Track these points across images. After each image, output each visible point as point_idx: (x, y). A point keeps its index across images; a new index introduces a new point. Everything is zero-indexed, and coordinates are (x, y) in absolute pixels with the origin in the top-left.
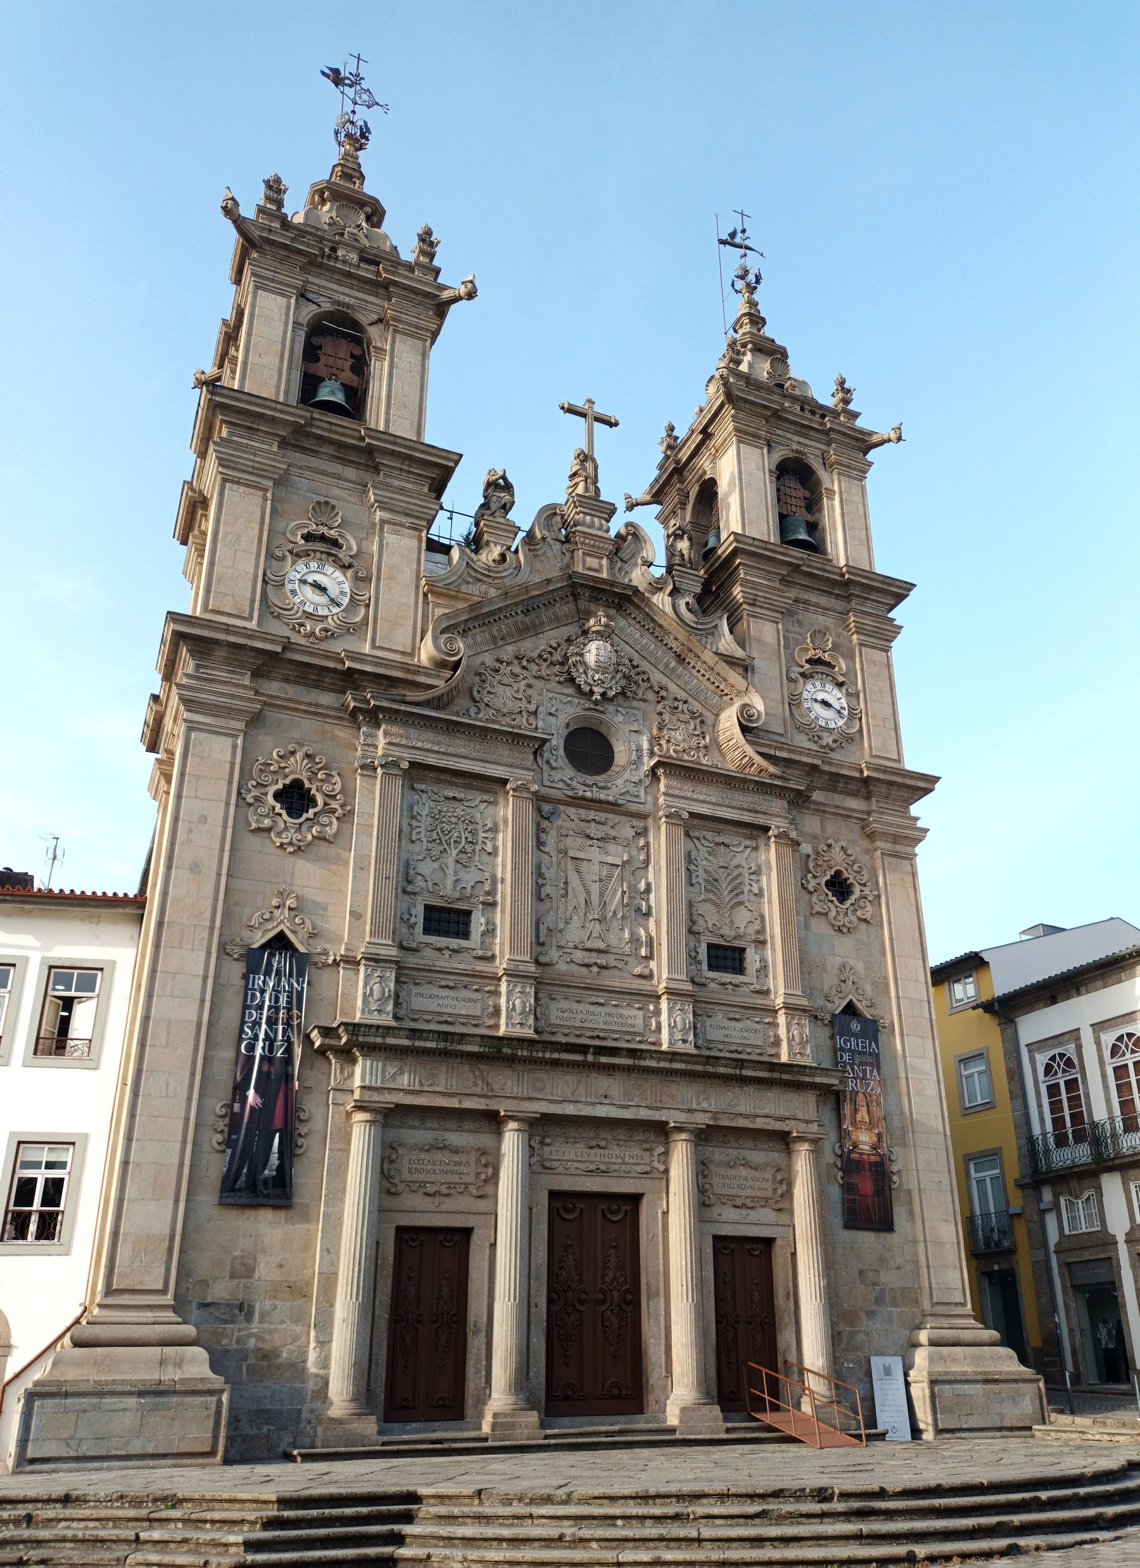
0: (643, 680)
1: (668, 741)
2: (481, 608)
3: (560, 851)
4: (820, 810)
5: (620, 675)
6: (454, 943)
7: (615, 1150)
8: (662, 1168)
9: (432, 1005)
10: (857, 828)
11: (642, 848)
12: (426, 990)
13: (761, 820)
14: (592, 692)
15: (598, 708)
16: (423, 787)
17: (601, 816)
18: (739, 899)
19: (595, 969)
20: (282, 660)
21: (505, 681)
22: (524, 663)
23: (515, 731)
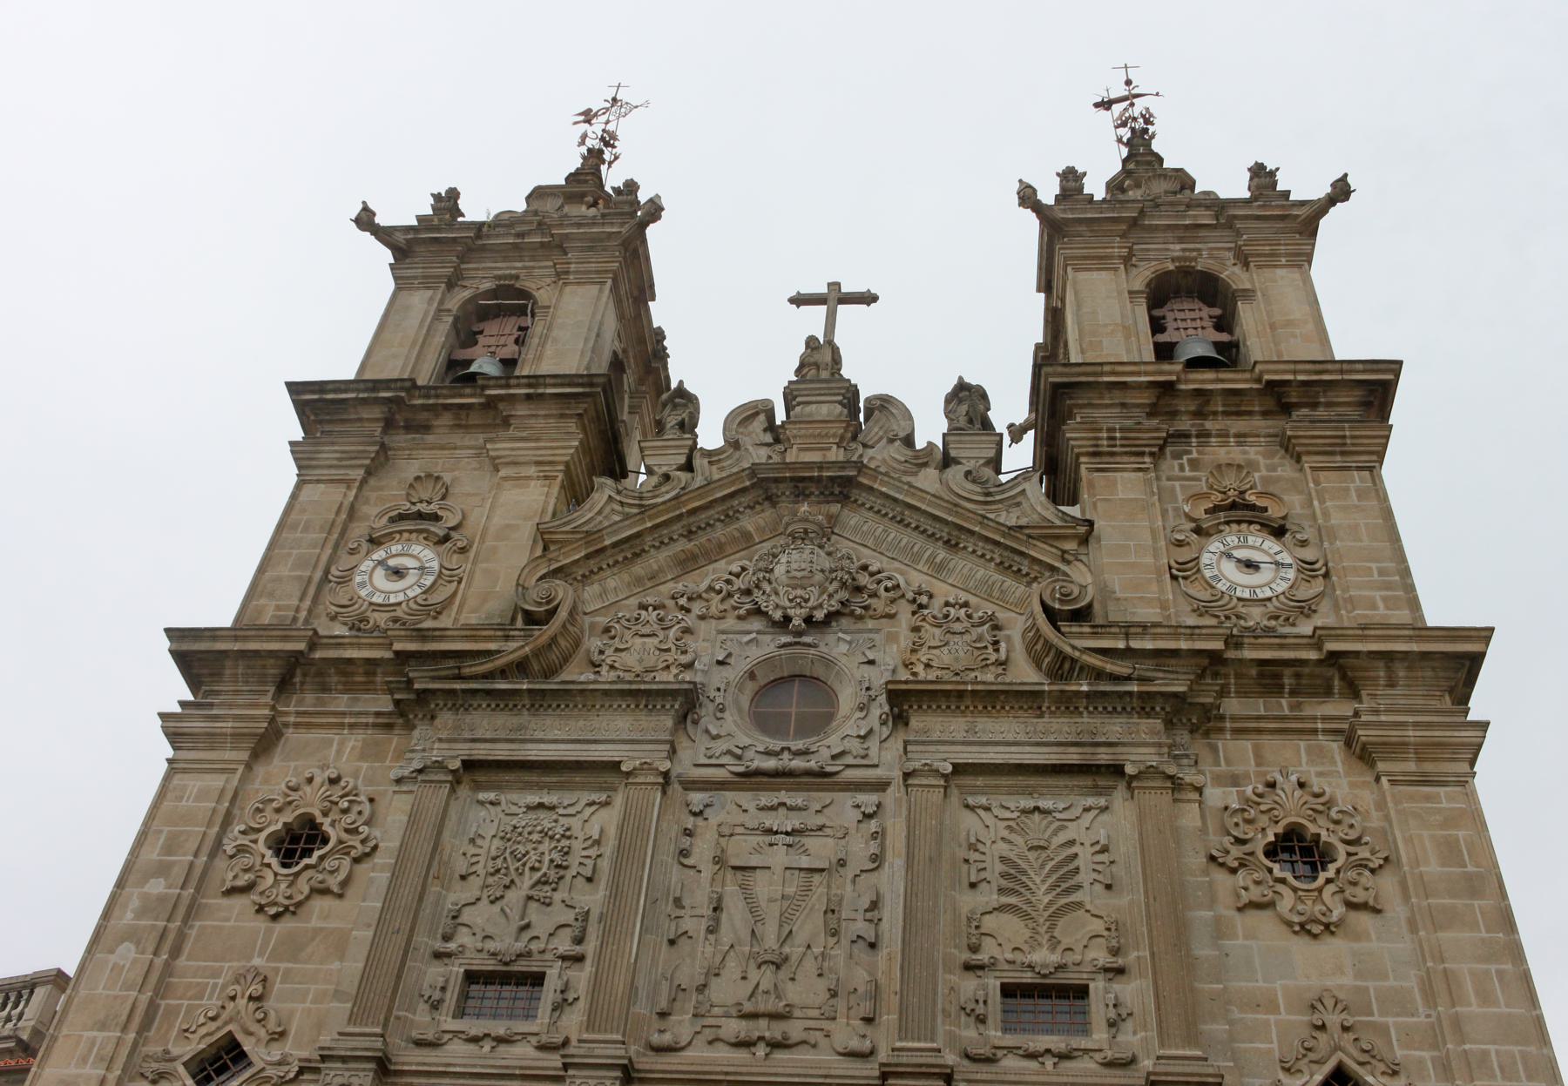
0: (887, 590)
1: (928, 666)
2: (601, 539)
3: (719, 861)
5: (835, 585)
10: (1335, 747)
11: (875, 836)
13: (1104, 756)
15: (807, 639)
16: (492, 796)
17: (796, 799)
18: (1073, 898)
19: (761, 1050)
20: (312, 662)
22: (683, 601)
23: (634, 687)
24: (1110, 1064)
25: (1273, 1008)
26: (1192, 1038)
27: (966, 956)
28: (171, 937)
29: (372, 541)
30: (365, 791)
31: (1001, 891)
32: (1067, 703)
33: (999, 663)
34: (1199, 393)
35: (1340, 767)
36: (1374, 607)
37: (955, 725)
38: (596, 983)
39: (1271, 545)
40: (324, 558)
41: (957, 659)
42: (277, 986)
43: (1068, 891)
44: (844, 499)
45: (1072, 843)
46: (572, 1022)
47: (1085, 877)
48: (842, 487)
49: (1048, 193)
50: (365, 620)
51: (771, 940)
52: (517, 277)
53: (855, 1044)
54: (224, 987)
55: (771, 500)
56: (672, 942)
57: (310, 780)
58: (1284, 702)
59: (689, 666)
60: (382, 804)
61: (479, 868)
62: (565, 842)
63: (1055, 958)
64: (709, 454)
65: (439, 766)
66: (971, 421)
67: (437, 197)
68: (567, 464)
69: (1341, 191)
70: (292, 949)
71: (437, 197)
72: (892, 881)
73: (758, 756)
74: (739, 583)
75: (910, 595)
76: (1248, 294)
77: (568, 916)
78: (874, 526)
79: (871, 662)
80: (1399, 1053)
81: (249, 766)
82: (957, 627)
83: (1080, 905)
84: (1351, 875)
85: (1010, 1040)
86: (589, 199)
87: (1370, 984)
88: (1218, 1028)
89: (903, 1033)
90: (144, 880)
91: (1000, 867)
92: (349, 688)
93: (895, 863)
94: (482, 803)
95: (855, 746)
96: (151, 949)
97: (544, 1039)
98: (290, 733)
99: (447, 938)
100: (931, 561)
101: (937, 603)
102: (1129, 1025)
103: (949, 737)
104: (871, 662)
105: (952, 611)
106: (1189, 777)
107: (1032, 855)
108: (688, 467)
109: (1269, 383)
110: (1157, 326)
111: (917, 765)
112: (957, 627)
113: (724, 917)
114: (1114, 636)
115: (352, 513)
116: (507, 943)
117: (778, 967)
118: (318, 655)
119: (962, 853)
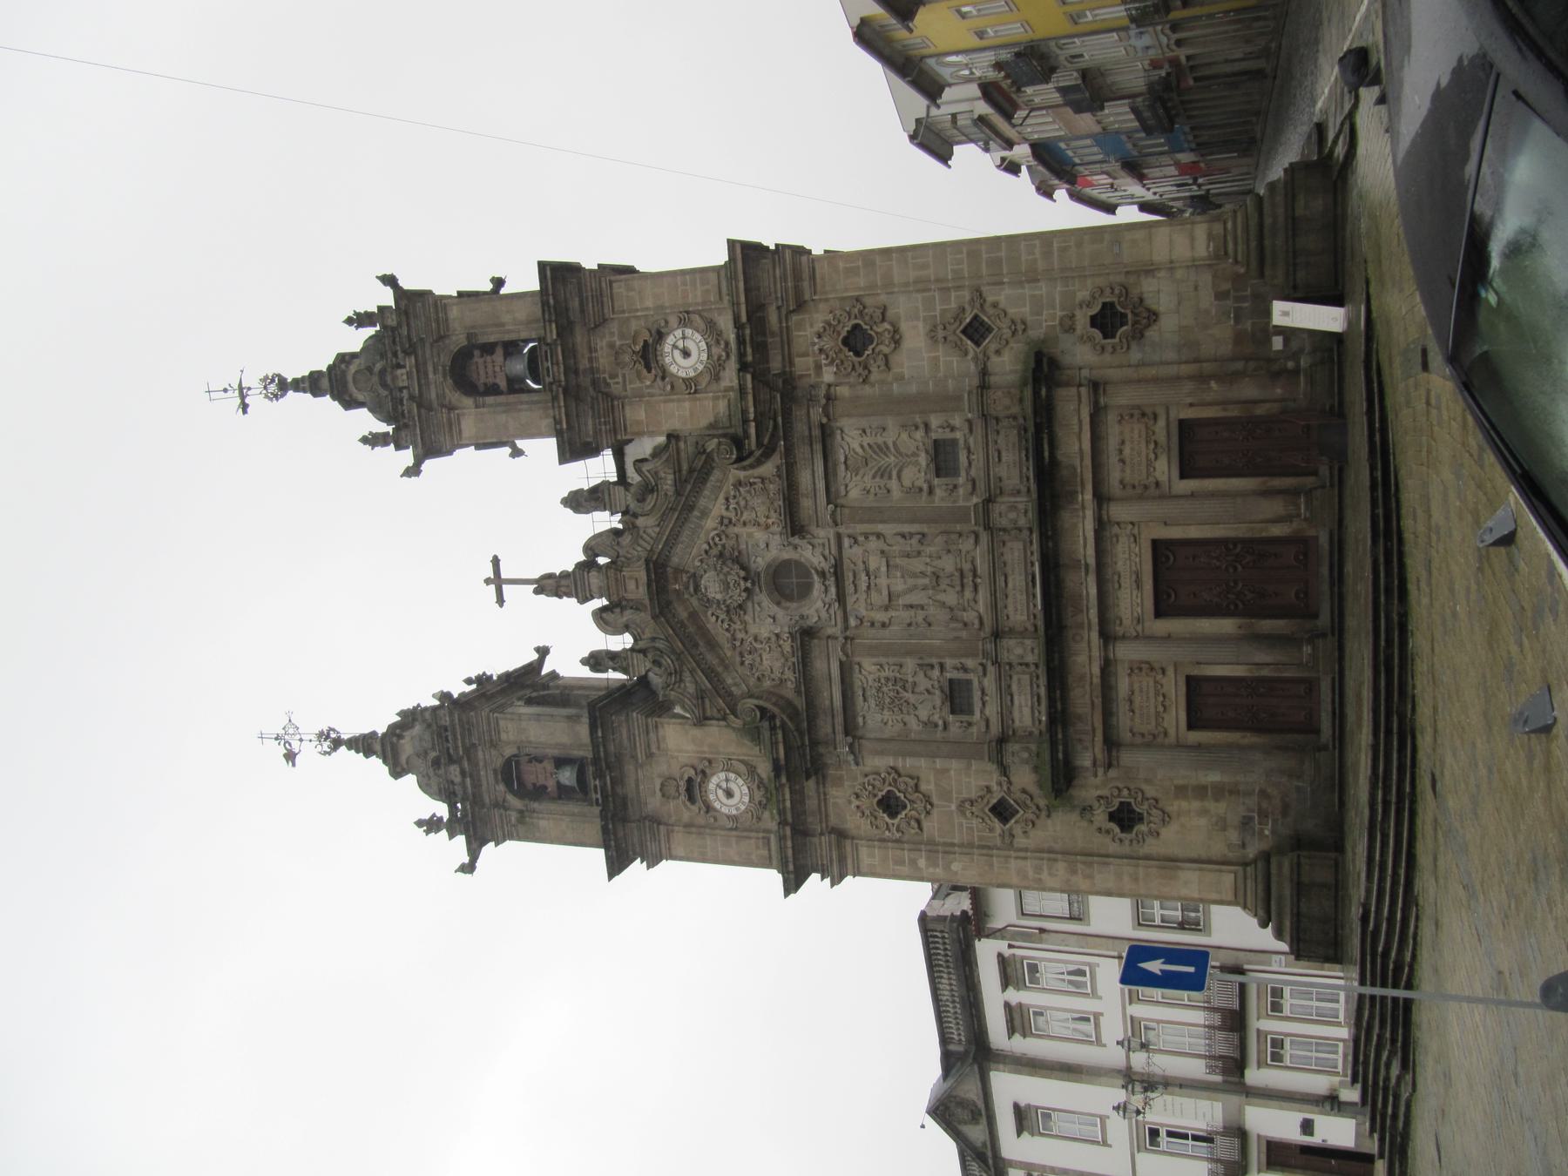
3: (886, 608)
6: (977, 695)
7: (1120, 566)
9: (1027, 711)
10: (795, 318)
12: (1016, 715)
13: (816, 432)
14: (746, 590)
17: (849, 577)
24: (971, 431)
25: (937, 359)
26: (959, 398)
27: (925, 493)
30: (861, 779)
31: (890, 478)
32: (789, 451)
37: (806, 503)
38: (953, 656)
39: (670, 340)
42: (965, 796)
44: (664, 566)
46: (970, 663)
47: (880, 440)
48: (658, 570)
51: (926, 581)
52: (495, 771)
53: (972, 540)
55: (669, 603)
60: (867, 769)
63: (923, 455)
64: (635, 640)
65: (851, 746)
66: (597, 499)
67: (428, 832)
69: (389, 280)
70: (946, 795)
71: (428, 832)
74: (723, 616)
76: (469, 336)
77: (921, 674)
78: (679, 549)
80: (953, 305)
82: (742, 503)
85: (963, 473)
88: (951, 384)
92: (802, 802)
93: (880, 528)
95: (818, 550)
99: (936, 725)
101: (725, 513)
103: (812, 503)
106: (823, 392)
108: (643, 652)
110: (493, 390)
112: (742, 503)
115: (688, 826)
116: (937, 698)
118: (790, 819)
119: (871, 497)
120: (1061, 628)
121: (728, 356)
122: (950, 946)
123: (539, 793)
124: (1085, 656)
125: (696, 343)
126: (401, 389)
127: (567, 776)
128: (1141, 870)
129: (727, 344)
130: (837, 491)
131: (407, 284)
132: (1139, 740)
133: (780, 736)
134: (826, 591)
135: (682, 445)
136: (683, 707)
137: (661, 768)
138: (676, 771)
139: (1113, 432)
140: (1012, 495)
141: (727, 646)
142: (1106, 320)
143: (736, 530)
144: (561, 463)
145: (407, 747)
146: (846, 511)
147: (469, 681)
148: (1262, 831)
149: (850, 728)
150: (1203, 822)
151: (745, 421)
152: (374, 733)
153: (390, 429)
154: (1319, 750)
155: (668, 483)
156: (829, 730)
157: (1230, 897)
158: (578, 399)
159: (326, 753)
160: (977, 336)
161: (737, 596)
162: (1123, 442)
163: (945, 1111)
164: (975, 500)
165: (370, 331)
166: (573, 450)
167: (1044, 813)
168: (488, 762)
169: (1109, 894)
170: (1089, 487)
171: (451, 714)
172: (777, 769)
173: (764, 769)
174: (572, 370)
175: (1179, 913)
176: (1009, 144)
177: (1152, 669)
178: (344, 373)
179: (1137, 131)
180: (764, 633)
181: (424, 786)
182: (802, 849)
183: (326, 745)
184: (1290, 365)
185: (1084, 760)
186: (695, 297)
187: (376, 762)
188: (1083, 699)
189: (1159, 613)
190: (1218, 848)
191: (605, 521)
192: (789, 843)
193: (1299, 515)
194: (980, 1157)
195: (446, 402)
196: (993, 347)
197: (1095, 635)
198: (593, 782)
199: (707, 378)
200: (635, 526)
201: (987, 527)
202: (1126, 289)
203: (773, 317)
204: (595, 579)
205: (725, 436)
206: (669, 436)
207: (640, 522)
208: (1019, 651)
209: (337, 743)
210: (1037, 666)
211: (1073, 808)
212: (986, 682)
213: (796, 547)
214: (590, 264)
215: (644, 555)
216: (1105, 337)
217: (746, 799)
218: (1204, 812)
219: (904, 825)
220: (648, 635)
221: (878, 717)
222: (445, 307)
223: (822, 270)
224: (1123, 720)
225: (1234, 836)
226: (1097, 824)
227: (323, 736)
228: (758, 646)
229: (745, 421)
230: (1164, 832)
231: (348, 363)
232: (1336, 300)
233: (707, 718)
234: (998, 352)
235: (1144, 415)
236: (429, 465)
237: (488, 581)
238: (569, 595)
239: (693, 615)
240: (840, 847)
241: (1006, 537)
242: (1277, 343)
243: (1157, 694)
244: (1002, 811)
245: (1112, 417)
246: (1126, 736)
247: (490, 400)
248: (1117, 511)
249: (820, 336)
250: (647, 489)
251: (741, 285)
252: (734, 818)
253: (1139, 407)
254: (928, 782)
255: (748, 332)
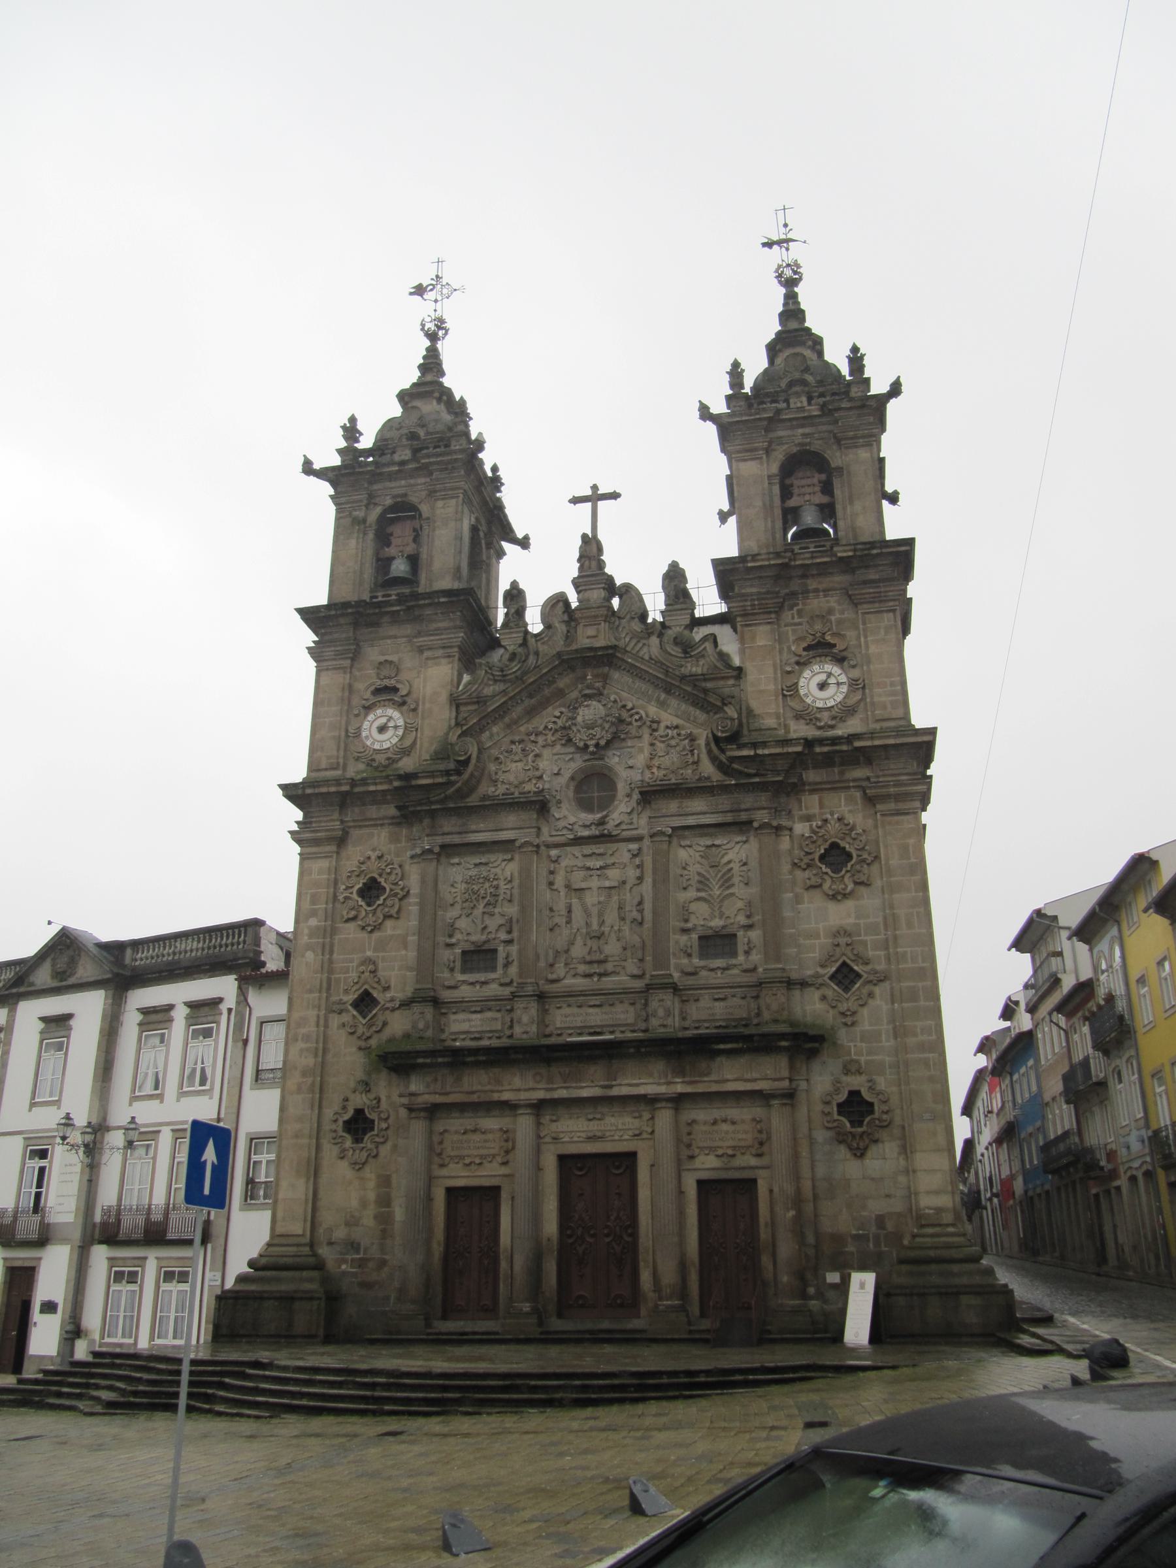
3: (568, 886)
4: (816, 789)
6: (482, 977)
7: (610, 1120)
8: (650, 1130)
9: (465, 1027)
10: (858, 795)
11: (638, 866)
12: (461, 1016)
13: (744, 817)
14: (586, 746)
17: (599, 849)
18: (731, 891)
21: (517, 758)
22: (533, 738)
24: (745, 971)
25: (818, 937)
26: (778, 959)
27: (683, 925)
28: (327, 947)
29: (364, 707)
30: (397, 861)
31: (698, 890)
32: (724, 789)
33: (694, 763)
34: (802, 566)
35: (860, 807)
36: (885, 708)
37: (673, 806)
38: (520, 952)
39: (836, 670)
40: (343, 723)
41: (673, 763)
42: (381, 965)
43: (728, 888)
44: (610, 664)
45: (729, 862)
46: (513, 970)
47: (736, 880)
48: (606, 659)
49: (719, 407)
50: (373, 760)
51: (595, 926)
52: (405, 495)
53: (636, 972)
54: (358, 967)
56: (551, 930)
57: (369, 858)
58: (836, 770)
59: (540, 777)
60: (407, 867)
61: (458, 899)
62: (495, 883)
64: (536, 635)
65: (430, 851)
66: (677, 597)
67: (344, 427)
68: (459, 647)
69: (895, 389)
70: (381, 946)
71: (344, 427)
72: (647, 887)
73: (581, 829)
75: (648, 723)
76: (840, 470)
77: (502, 921)
78: (627, 679)
79: (631, 767)
81: (338, 853)
82: (673, 742)
83: (733, 894)
84: (858, 867)
85: (703, 963)
86: (437, 395)
87: (862, 921)
89: (655, 968)
90: (307, 920)
91: (697, 878)
93: (648, 880)
94: (453, 864)
95: (625, 818)
96: (320, 953)
97: (502, 981)
98: (352, 831)
99: (451, 936)
100: (658, 700)
101: (662, 725)
102: (754, 952)
104: (631, 767)
105: (670, 731)
106: (784, 823)
107: (711, 870)
108: (524, 643)
109: (841, 558)
110: (786, 492)
111: (655, 830)
112: (673, 742)
113: (573, 916)
114: (750, 749)
116: (478, 937)
117: (599, 938)
118: (357, 790)
119: (679, 871)
120: (548, 1061)
121: (820, 728)
122: (230, 950)
123: (383, 538)
124: (520, 1085)
125: (833, 696)
126: (787, 401)
127: (399, 567)
128: (305, 1141)
129: (832, 727)
130: (684, 838)
131: (892, 406)
132: (436, 1139)
133: (440, 780)
134: (585, 826)
135: (731, 682)
136: (469, 683)
137: (408, 661)
138: (404, 676)
139: (744, 1113)
140: (681, 1012)
141: (530, 727)
142: (856, 1107)
143: (646, 737)
144: (713, 560)
145: (429, 407)
146: (665, 846)
147: (495, 469)
148: (345, 1261)
149: (448, 850)
150: (355, 1203)
151: (755, 745)
152: (443, 374)
153: (747, 389)
154: (426, 1319)
155: (693, 668)
156: (446, 829)
157: (279, 1230)
158: (777, 578)
159: (423, 325)
160: (840, 976)
161: (580, 737)
162: (733, 1123)
163: (65, 946)
164: (676, 975)
165: (845, 370)
166: (726, 572)
167: (363, 1044)
168: (414, 489)
169: (283, 1109)
170: (689, 1089)
171: (462, 451)
172: (407, 777)
173: (407, 764)
174: (806, 572)
175: (263, 1179)
176: (1032, 1009)
177: (507, 1152)
178: (803, 344)
179: (1045, 1137)
180: (543, 764)
181: (390, 424)
182: (326, 802)
183: (430, 326)
184: (811, 1290)
185: (416, 1084)
186: (880, 695)
187: (414, 376)
188: (477, 1083)
189: (563, 1159)
190: (328, 1218)
191: (655, 605)
192: (333, 789)
193: (660, 1299)
194: (19, 980)
195: (773, 446)
196: (829, 993)
197: (541, 1095)
198: (394, 593)
199: (798, 707)
200: (650, 634)
201: (649, 987)
202: (888, 1125)
203: (859, 773)
204: (597, 595)
205: (741, 725)
206: (740, 669)
207: (654, 640)
208: (525, 1019)
209: (433, 337)
210: (511, 1037)
211: (369, 1074)
212: (494, 986)
213: (629, 796)
214: (912, 590)
215: (621, 644)
216: (839, 1105)
217: (377, 746)
218: (364, 1204)
219: (351, 903)
220: (542, 648)
221: (459, 878)
222: (869, 445)
223: (906, 822)
224: (456, 1123)
225: (340, 1234)
226: (352, 1097)
227: (440, 323)
228: (530, 758)
229: (755, 745)
230: (344, 1165)
231: (813, 348)
232: (876, 1335)
233: (458, 707)
234: (824, 998)
235: (761, 1144)
236: (711, 429)
237: (595, 488)
238: (581, 569)
239: (561, 693)
240: (329, 840)
241: (638, 1006)
242: (833, 1277)
243: (481, 1157)
244: (365, 1002)
245: (758, 1111)
246: (440, 1126)
247: (776, 490)
248: (665, 1117)
249: (839, 820)
250: (687, 648)
251: (891, 741)
252: (358, 734)
253: (769, 1138)
254: (394, 928)
255: (845, 748)
